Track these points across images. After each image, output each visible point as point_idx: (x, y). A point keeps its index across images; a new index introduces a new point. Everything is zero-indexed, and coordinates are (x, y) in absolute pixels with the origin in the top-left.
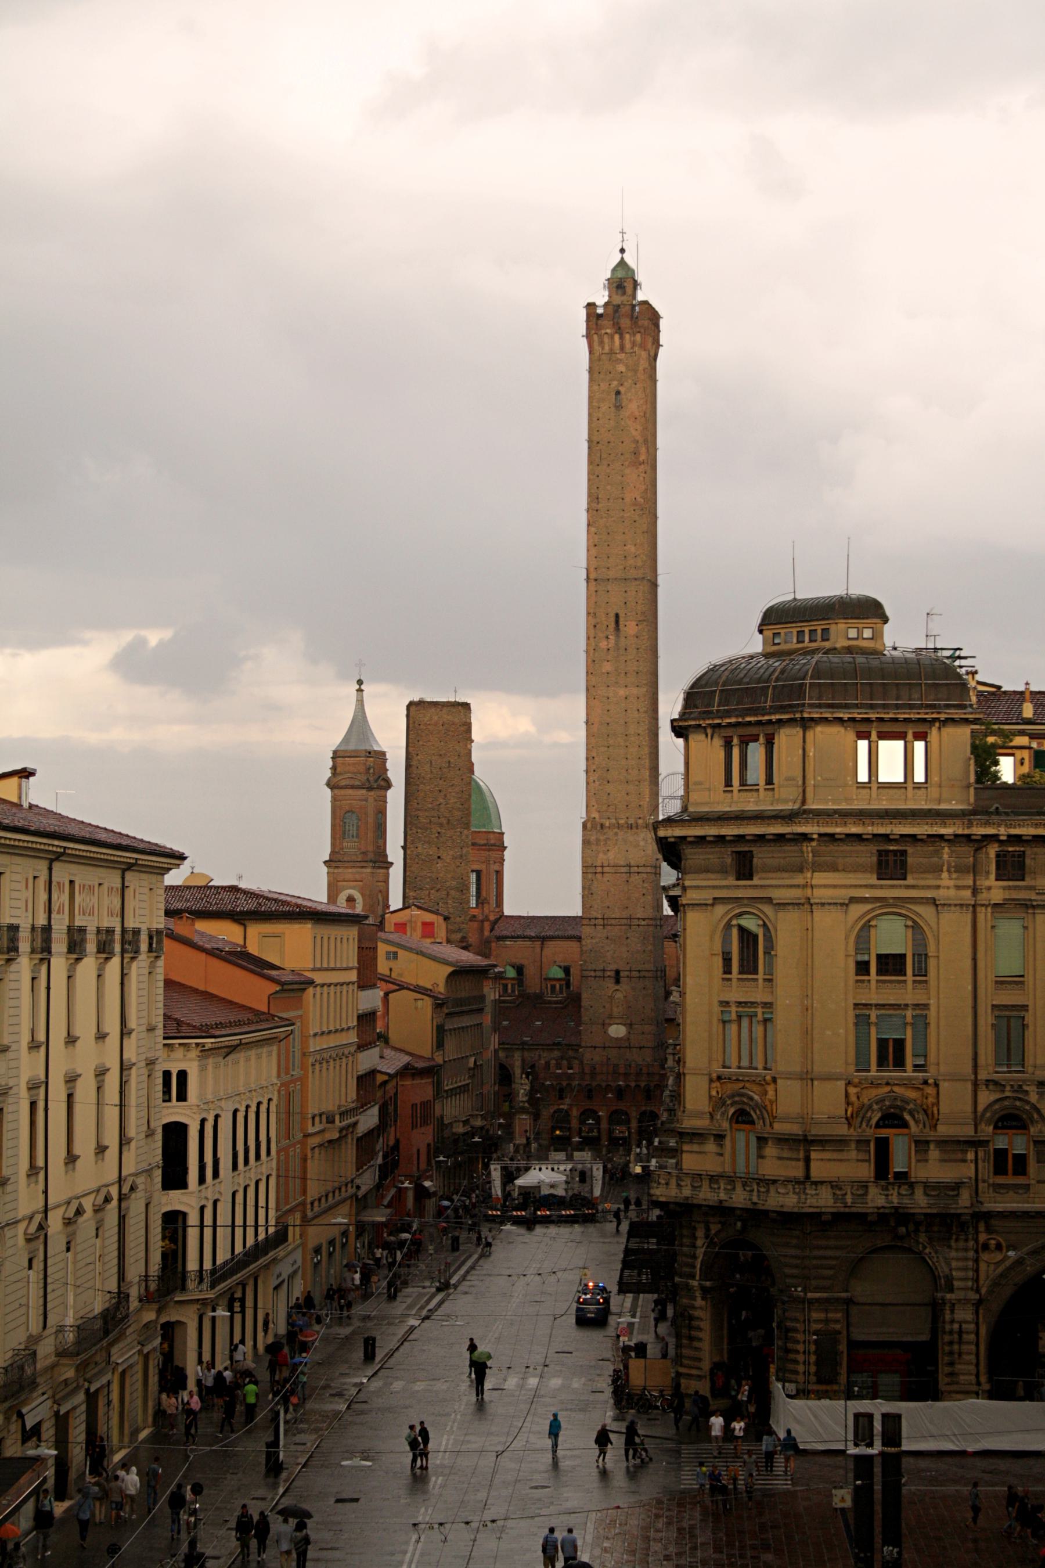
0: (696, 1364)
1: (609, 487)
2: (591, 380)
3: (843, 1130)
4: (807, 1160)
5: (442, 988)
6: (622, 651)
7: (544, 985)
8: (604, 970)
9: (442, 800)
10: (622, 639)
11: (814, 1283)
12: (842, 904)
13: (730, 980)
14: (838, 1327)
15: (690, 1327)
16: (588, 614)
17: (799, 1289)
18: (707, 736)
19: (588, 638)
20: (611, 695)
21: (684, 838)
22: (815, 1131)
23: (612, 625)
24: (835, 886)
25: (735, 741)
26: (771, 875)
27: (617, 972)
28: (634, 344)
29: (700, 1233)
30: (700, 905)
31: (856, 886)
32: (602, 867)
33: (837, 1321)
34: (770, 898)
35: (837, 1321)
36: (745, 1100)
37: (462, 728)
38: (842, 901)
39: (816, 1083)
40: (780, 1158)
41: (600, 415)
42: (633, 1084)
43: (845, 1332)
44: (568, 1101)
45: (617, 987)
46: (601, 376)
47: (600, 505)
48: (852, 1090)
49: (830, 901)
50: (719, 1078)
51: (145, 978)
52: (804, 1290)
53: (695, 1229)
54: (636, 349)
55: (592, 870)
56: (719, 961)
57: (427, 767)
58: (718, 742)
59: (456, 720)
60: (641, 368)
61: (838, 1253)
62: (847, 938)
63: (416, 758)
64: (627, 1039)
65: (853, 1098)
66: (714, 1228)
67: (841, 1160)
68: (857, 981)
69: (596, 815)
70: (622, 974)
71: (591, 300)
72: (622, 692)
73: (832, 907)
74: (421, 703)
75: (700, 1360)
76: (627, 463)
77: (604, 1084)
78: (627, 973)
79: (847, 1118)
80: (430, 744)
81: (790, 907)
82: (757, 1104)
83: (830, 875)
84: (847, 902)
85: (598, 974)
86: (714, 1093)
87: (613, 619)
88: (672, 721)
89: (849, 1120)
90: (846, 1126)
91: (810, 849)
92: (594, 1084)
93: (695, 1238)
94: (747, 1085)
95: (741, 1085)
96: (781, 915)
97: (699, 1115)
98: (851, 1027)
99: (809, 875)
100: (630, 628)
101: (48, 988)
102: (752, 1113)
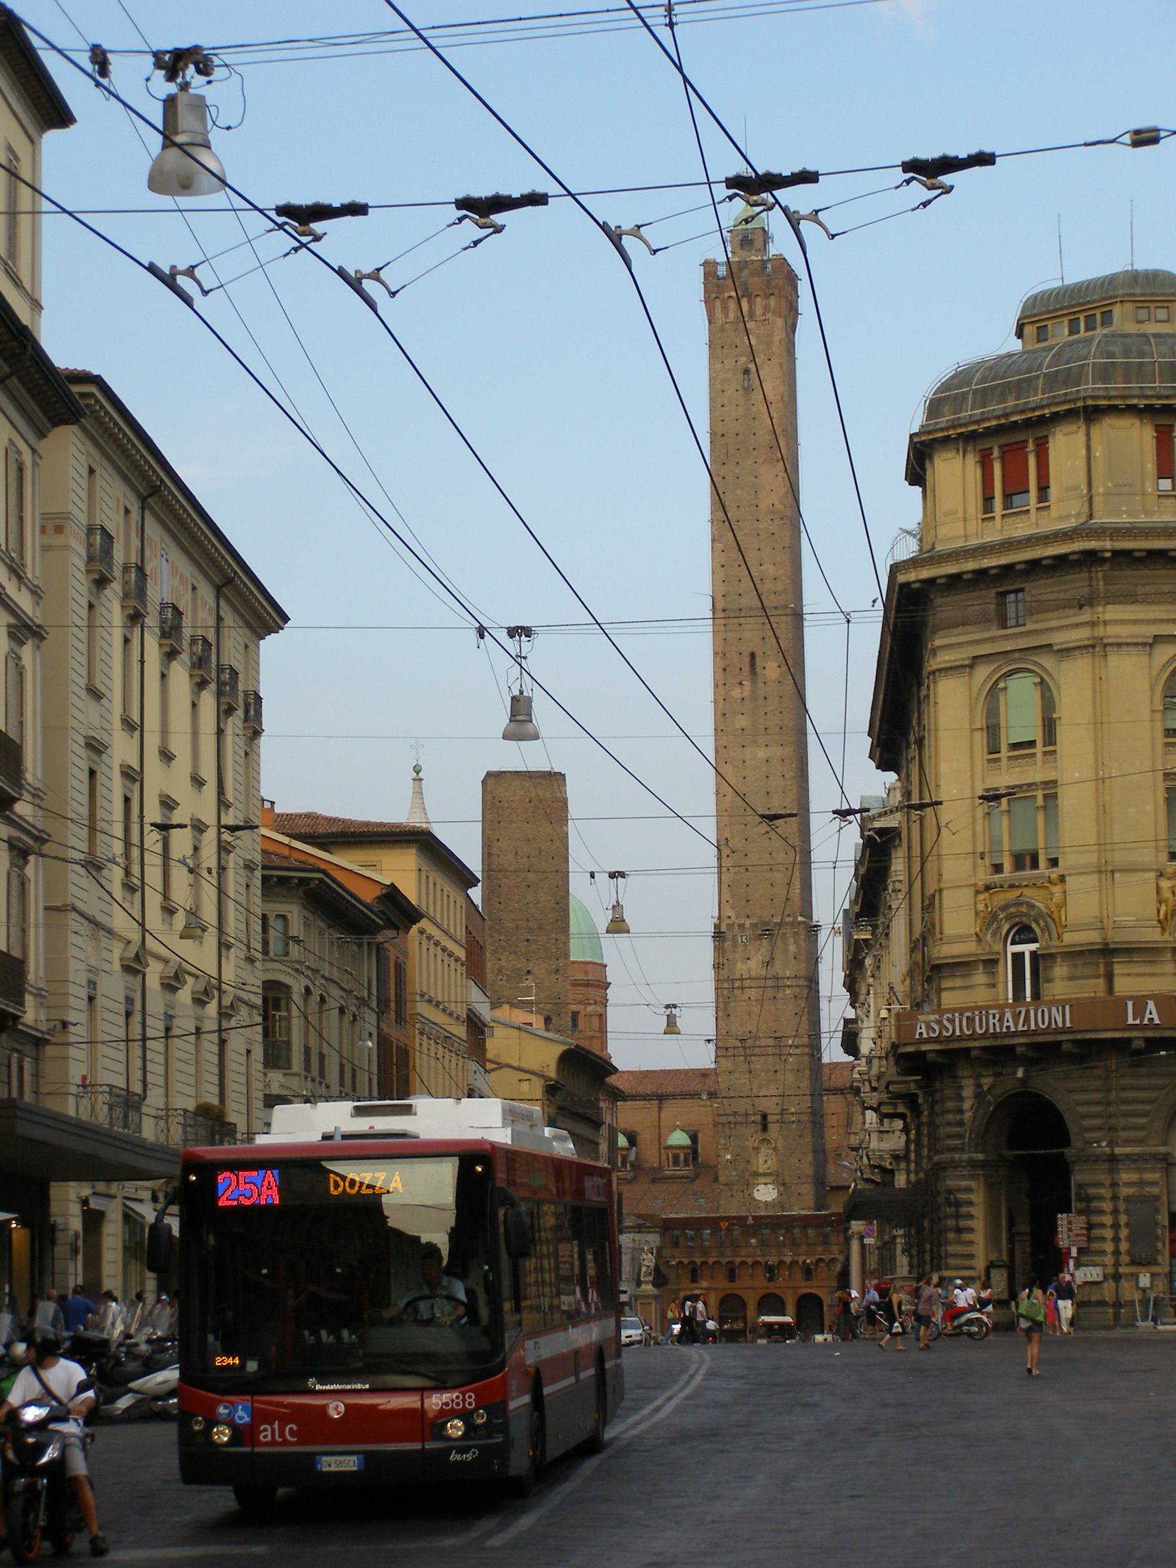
0: (968, 1262)
1: (738, 492)
2: (713, 357)
3: (1153, 935)
4: (1109, 977)
5: (552, 1073)
6: (761, 701)
7: (664, 1157)
8: (747, 1115)
9: (530, 898)
10: (761, 685)
11: (1124, 1134)
12: (1144, 644)
13: (998, 760)
14: (1155, 1191)
15: (958, 1216)
16: (716, 654)
17: (1104, 1144)
18: (958, 451)
19: (716, 686)
20: (748, 757)
21: (931, 582)
22: (1117, 938)
23: (747, 668)
24: (1134, 622)
25: (996, 453)
26: (1052, 615)
28: (766, 308)
29: (968, 1092)
30: (956, 667)
31: (1161, 621)
33: (1154, 1184)
34: (1050, 645)
35: (1154, 1184)
36: (1024, 909)
37: (555, 805)
38: (1145, 640)
39: (1117, 875)
40: (1072, 978)
41: (726, 401)
42: (788, 1259)
43: (1165, 1198)
46: (725, 351)
48: (1165, 884)
49: (1129, 640)
50: (988, 888)
51: (241, 761)
52: (1111, 1144)
53: (961, 1087)
54: (769, 316)
56: (980, 739)
57: (511, 857)
58: (972, 460)
59: (548, 794)
60: (776, 339)
61: (1152, 1094)
62: (1152, 689)
63: (497, 844)
64: (780, 1203)
65: (1167, 894)
66: (986, 1082)
67: (1154, 975)
68: (1167, 744)
69: (732, 914)
70: (770, 1118)
71: (710, 256)
72: (762, 753)
73: (1131, 648)
74: (500, 774)
75: (971, 1256)
76: (760, 461)
77: (750, 1260)
79: (1159, 921)
80: (514, 825)
81: (1077, 652)
82: (1040, 914)
83: (1128, 608)
84: (1151, 641)
85: (739, 1119)
86: (981, 907)
87: (747, 659)
88: (911, 436)
89: (1162, 924)
90: (1159, 930)
91: (1100, 574)
92: (738, 1260)
93: (961, 1099)
94: (1026, 891)
95: (1017, 893)
96: (1065, 665)
97: (961, 939)
98: (1161, 803)
99: (1100, 609)
100: (771, 670)
101: (142, 662)
102: (1034, 926)
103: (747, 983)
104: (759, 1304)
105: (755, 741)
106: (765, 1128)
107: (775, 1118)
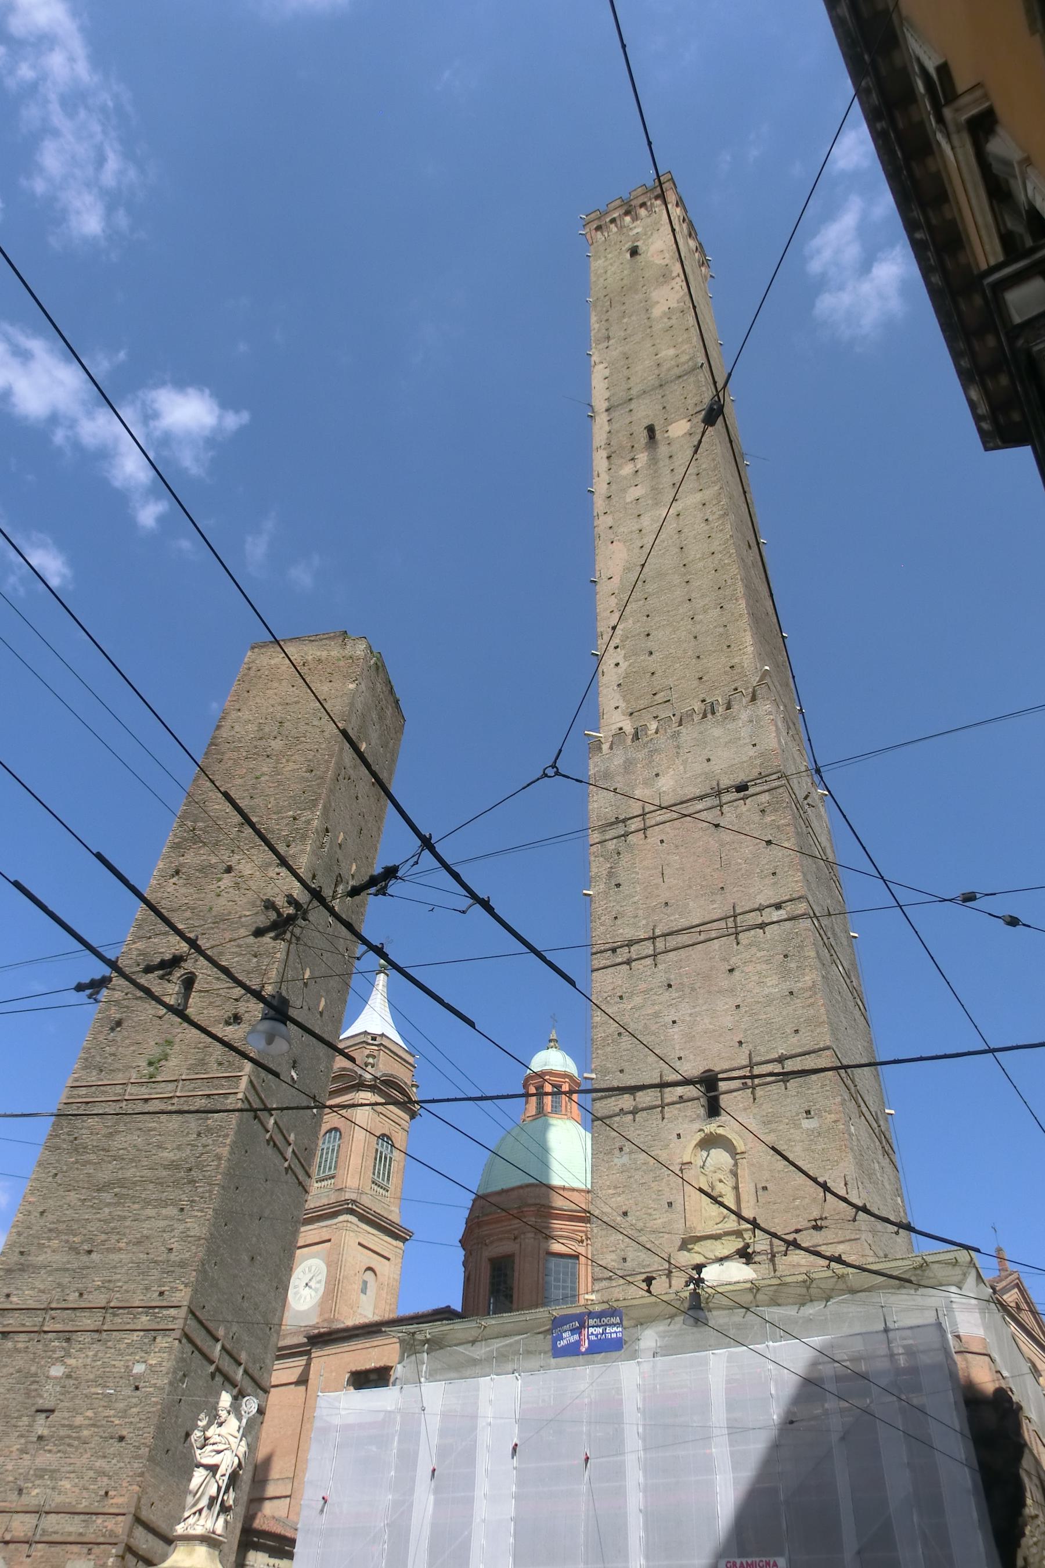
1: (625, 320)
10: (663, 450)
20: (645, 524)
37: (342, 663)
45: (712, 1127)
47: (611, 342)
55: (620, 830)
87: (643, 437)
105: (657, 504)
106: (714, 1109)
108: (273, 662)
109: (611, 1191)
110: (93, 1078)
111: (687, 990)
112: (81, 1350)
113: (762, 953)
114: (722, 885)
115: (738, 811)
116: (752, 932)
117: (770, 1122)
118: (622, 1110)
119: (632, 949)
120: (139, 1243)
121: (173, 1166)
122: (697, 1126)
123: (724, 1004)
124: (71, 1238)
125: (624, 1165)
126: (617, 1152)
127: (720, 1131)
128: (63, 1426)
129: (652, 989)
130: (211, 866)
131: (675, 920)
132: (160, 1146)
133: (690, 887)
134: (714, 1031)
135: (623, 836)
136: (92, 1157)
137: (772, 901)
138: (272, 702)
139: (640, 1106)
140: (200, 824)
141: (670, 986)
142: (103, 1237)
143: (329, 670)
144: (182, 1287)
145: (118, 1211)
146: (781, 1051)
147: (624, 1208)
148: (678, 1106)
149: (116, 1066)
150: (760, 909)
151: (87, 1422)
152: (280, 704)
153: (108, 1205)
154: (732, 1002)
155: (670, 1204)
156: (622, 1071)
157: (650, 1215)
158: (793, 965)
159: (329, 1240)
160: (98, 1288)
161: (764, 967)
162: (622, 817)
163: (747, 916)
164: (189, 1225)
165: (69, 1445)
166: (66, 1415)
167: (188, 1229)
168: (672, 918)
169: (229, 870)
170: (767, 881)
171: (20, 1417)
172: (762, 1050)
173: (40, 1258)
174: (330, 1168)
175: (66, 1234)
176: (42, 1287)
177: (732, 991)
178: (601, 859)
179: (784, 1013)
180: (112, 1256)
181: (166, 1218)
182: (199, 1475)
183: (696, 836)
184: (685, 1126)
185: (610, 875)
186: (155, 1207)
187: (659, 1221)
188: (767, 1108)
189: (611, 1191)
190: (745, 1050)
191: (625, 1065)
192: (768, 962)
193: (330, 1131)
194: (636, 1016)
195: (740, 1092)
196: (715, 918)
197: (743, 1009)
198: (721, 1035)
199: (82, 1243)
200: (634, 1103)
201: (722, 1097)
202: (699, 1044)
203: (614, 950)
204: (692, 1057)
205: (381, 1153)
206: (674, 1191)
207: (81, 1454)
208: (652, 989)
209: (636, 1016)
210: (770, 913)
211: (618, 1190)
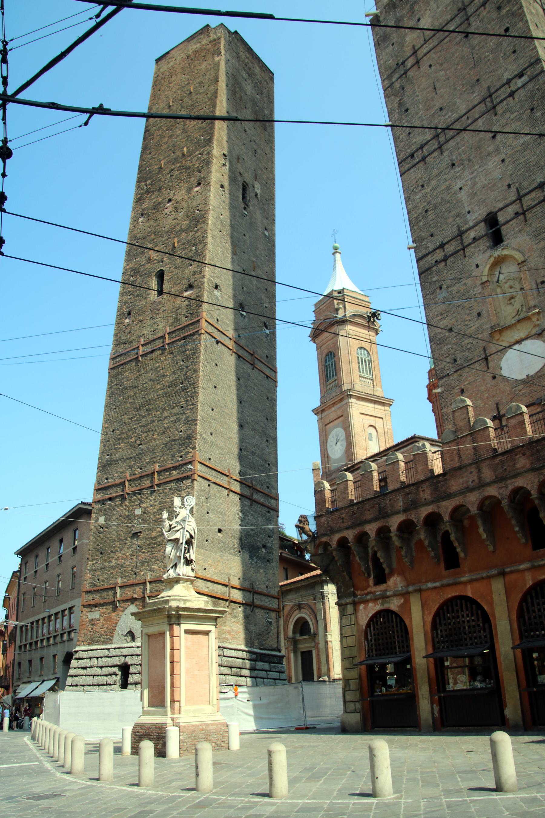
27: (492, 221)
32: (415, 52)
37: (210, 46)
44: (395, 582)
45: (499, 252)
70: (501, 218)
77: (472, 500)
78: (516, 207)
85: (450, 248)
92: (446, 508)
103: (420, 54)
104: (521, 614)
106: (497, 239)
107: (511, 210)
108: (170, 65)
109: (439, 318)
110: (121, 350)
111: (466, 163)
112: (147, 498)
113: (515, 115)
114: (477, 78)
115: (481, 17)
116: (505, 102)
117: (539, 234)
118: (436, 261)
119: (424, 150)
120: (163, 433)
121: (172, 384)
122: (488, 254)
123: (493, 163)
124: (130, 441)
125: (444, 298)
126: (438, 291)
127: (505, 252)
128: (148, 538)
129: (442, 172)
130: (159, 203)
131: (449, 117)
132: (164, 376)
133: (455, 89)
134: (489, 184)
135: (404, 74)
136: (131, 393)
137: (516, 73)
138: (174, 90)
139: (448, 254)
140: (149, 182)
141: (453, 165)
142: (145, 435)
143: (203, 54)
144: (191, 450)
145: (149, 418)
146: (539, 181)
147: (449, 326)
148: (473, 245)
149: (132, 338)
150: (509, 82)
151: (158, 534)
152: (179, 89)
153: (144, 417)
154: (498, 159)
155: (479, 314)
156: (432, 235)
157: (467, 325)
158: (539, 114)
159: (342, 416)
160: (148, 463)
161: (518, 124)
162: (400, 62)
163: (499, 92)
164: (188, 415)
165: (152, 547)
166: (147, 533)
167: (188, 417)
168: (447, 117)
169: (170, 200)
170: (509, 60)
171: (126, 539)
172: (525, 184)
173: (117, 456)
174: (333, 376)
175: (127, 439)
176: (121, 470)
177: (497, 151)
178: (393, 97)
179: (538, 152)
180: (152, 444)
181: (175, 414)
182: (169, 548)
183: (453, 50)
184: (481, 257)
185: (400, 105)
186: (168, 410)
187: (474, 328)
188: (536, 225)
189: (439, 318)
190: (513, 189)
191: (434, 230)
192: (519, 119)
193: (327, 355)
194: (435, 194)
195: (515, 220)
196: (476, 103)
197: (507, 161)
198: (494, 185)
199: (135, 442)
200: (443, 254)
201: (503, 228)
202: (481, 197)
203: (412, 156)
204: (476, 208)
205: (362, 359)
206: (481, 304)
207: (159, 551)
208: (442, 172)
209: (435, 194)
210: (516, 83)
211: (445, 315)
